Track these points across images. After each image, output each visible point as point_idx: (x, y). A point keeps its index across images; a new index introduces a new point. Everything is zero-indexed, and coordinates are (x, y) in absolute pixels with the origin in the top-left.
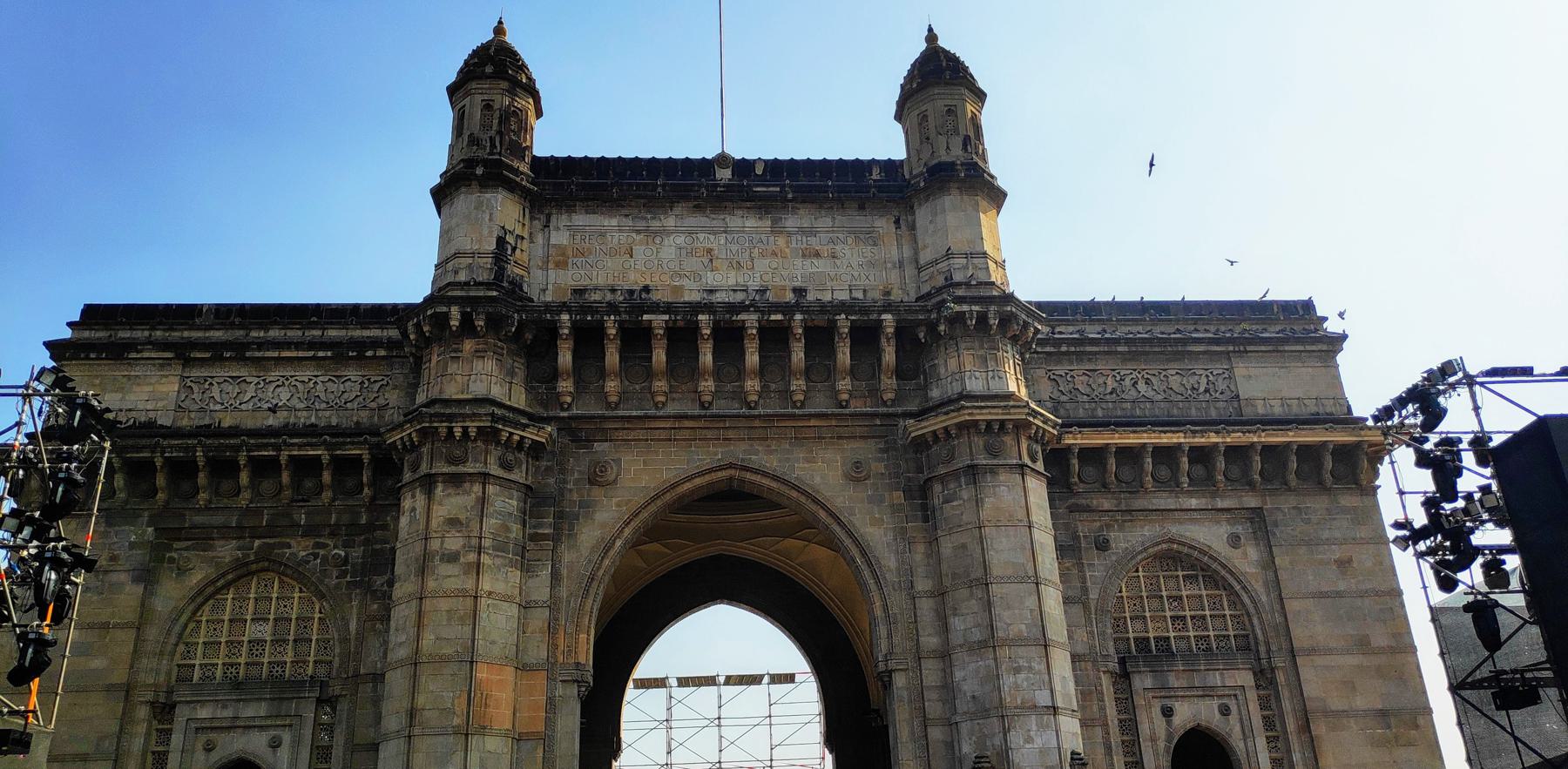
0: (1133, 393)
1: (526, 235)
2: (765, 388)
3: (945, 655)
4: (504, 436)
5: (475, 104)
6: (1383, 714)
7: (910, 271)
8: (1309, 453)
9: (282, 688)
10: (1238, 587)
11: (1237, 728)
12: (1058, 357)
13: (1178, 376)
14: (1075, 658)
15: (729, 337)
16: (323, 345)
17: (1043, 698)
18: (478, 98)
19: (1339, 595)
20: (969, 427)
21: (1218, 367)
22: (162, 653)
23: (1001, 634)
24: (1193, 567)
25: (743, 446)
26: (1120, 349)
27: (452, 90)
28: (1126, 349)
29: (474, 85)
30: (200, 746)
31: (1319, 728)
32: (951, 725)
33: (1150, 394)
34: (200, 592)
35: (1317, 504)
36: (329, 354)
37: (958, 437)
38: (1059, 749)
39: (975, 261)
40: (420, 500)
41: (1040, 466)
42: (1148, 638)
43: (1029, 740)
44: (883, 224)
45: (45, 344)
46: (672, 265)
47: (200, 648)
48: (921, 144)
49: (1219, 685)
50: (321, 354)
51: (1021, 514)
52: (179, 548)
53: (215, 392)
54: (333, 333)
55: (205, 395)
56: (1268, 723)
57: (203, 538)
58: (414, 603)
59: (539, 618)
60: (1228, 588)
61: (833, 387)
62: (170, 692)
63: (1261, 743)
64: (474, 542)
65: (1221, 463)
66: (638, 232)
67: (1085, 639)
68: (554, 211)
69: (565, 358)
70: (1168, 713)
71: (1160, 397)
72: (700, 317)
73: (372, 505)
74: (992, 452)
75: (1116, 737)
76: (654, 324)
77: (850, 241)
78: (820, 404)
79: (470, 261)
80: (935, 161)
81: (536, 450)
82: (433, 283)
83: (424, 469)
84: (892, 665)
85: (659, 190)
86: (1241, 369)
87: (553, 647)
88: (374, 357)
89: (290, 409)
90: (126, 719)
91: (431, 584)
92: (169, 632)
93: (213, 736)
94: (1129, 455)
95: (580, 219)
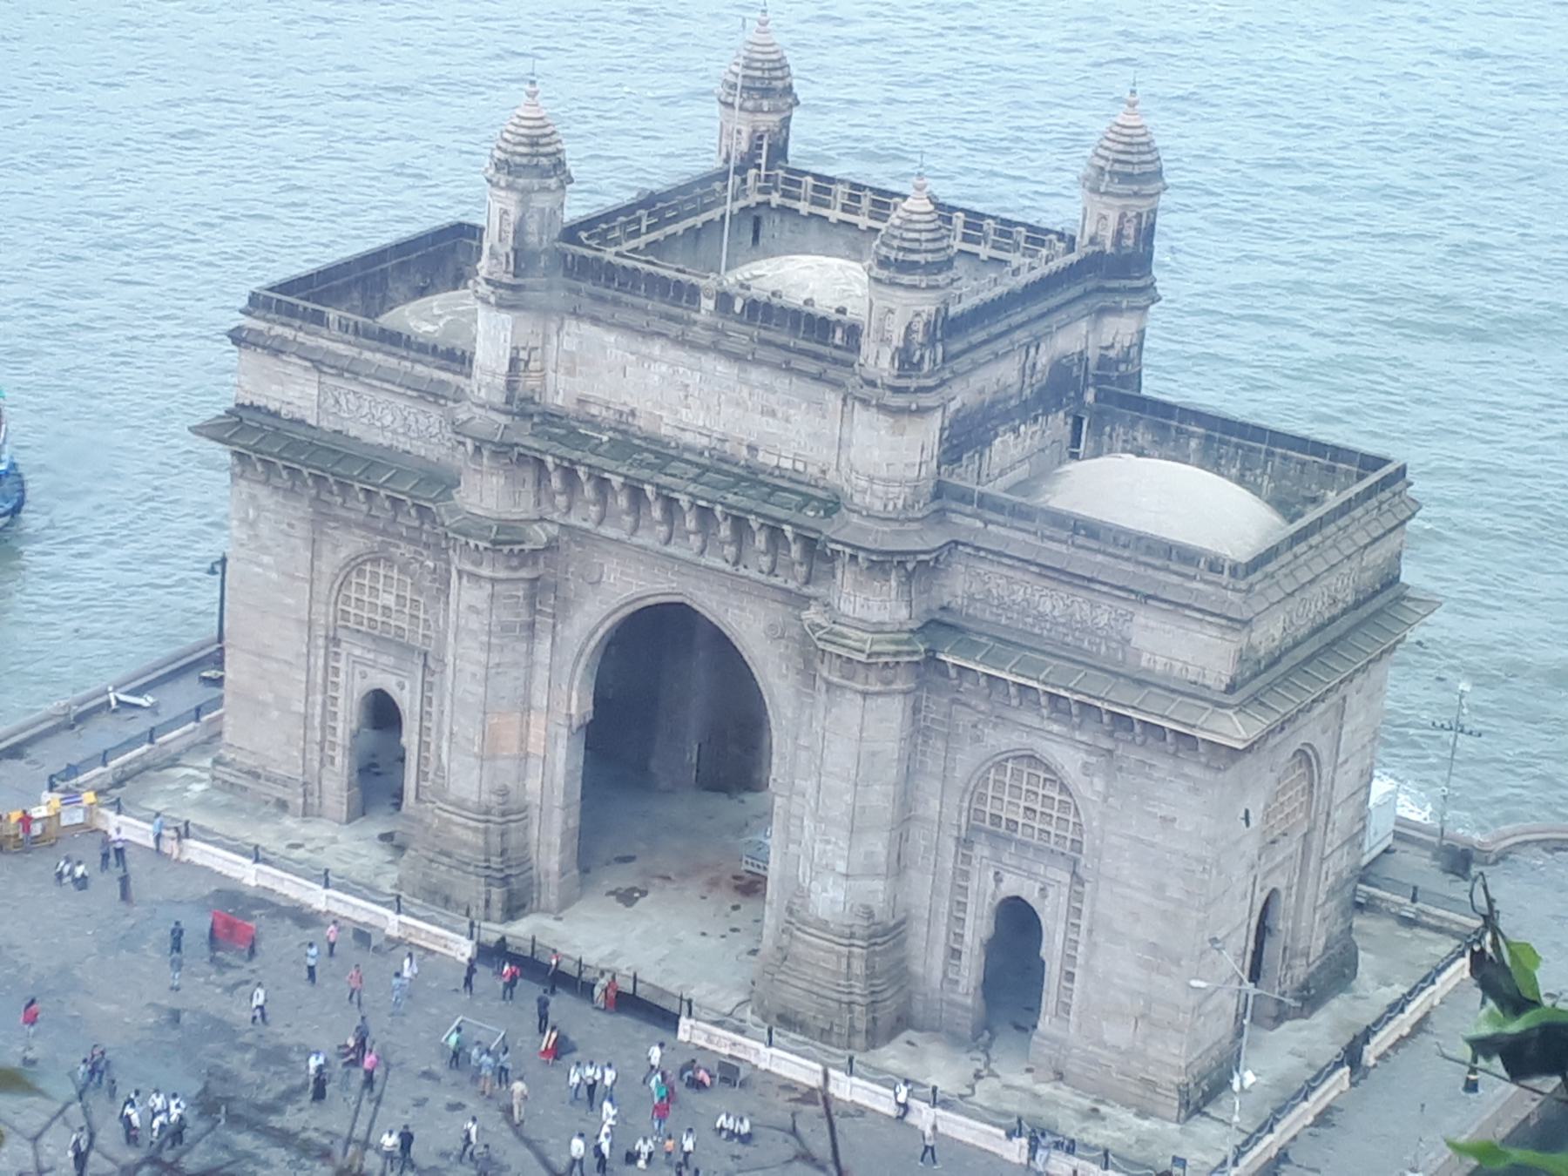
6: (1153, 948)
17: (841, 867)
19: (1153, 845)
21: (1124, 607)
31: (1100, 938)
63: (1061, 926)
70: (998, 879)
77: (804, 406)
86: (1140, 619)
95: (587, 328)
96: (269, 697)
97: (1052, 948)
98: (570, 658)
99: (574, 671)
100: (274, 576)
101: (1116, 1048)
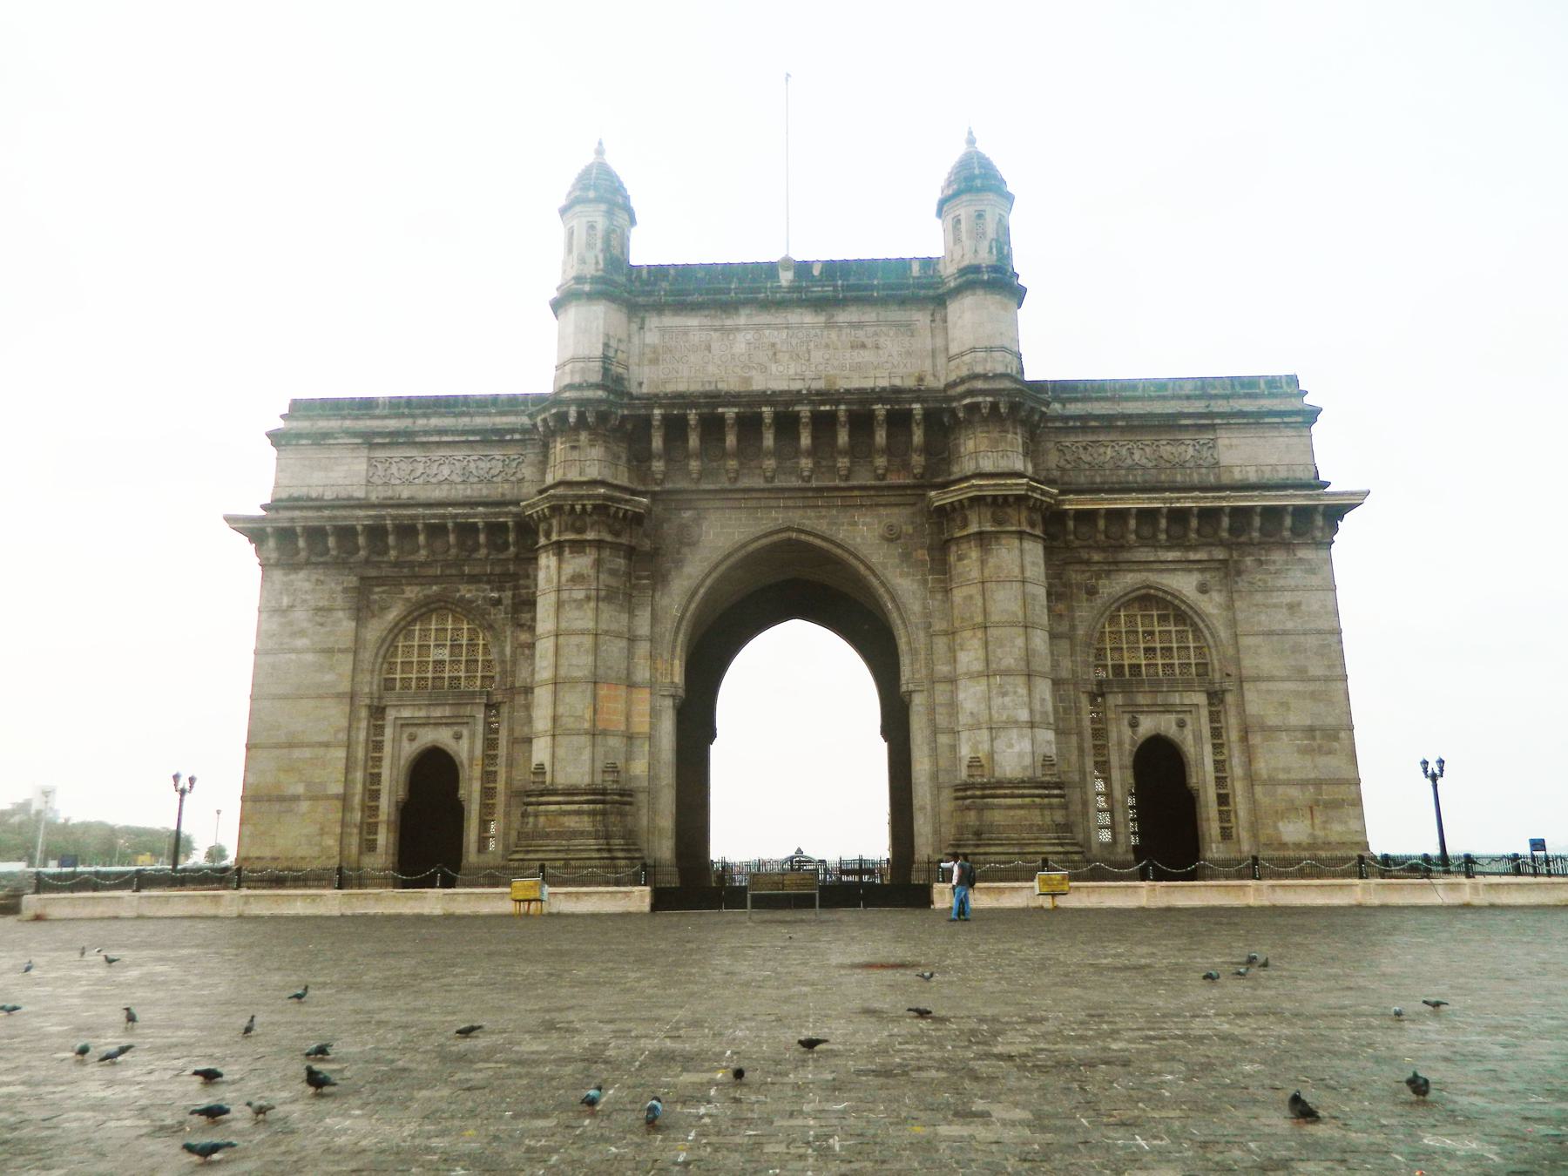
0: (1129, 462)
1: (624, 337)
2: (817, 464)
3: (952, 680)
4: (612, 510)
5: (580, 225)
6: (1310, 731)
7: (941, 360)
9: (461, 697)
10: (1201, 625)
11: (1190, 737)
12: (1068, 430)
13: (1169, 448)
14: (1057, 683)
16: (473, 432)
17: (1024, 715)
18: (584, 220)
19: (1285, 633)
20: (977, 501)
21: (1205, 437)
22: (372, 671)
23: (994, 666)
24: (1166, 608)
25: (800, 512)
26: (1119, 423)
27: (563, 211)
28: (1123, 423)
30: (405, 736)
31: (1256, 739)
32: (955, 733)
33: (1144, 461)
34: (397, 624)
35: (1278, 556)
36: (478, 438)
37: (971, 507)
38: (1033, 753)
39: (994, 354)
40: (553, 561)
41: (1038, 532)
42: (1122, 666)
44: (921, 318)
46: (742, 359)
47: (399, 667)
48: (955, 244)
49: (1178, 702)
50: (471, 438)
51: (1017, 571)
52: (378, 593)
53: (394, 469)
54: (480, 421)
55: (389, 472)
56: (1216, 733)
57: (395, 583)
58: (552, 640)
59: (643, 648)
60: (1194, 625)
61: (871, 462)
62: (380, 698)
63: (1208, 749)
64: (593, 593)
65: (1194, 523)
66: (716, 330)
67: (1070, 665)
68: (647, 315)
69: (657, 443)
70: (1134, 725)
71: (1150, 465)
72: (764, 409)
73: (517, 558)
74: (997, 521)
75: (1089, 743)
77: (891, 333)
78: (863, 478)
79: (582, 364)
80: (966, 263)
81: (637, 519)
82: (555, 381)
83: (554, 537)
84: (911, 687)
85: (733, 294)
86: (1224, 439)
87: (653, 669)
88: (511, 440)
89: (452, 482)
90: (352, 717)
91: (563, 625)
92: (377, 654)
93: (413, 730)
94: (1118, 516)
95: (670, 320)
96: (300, 789)
97: (1202, 775)
98: (667, 626)
99: (675, 640)
100: (310, 657)
101: (1298, 846)
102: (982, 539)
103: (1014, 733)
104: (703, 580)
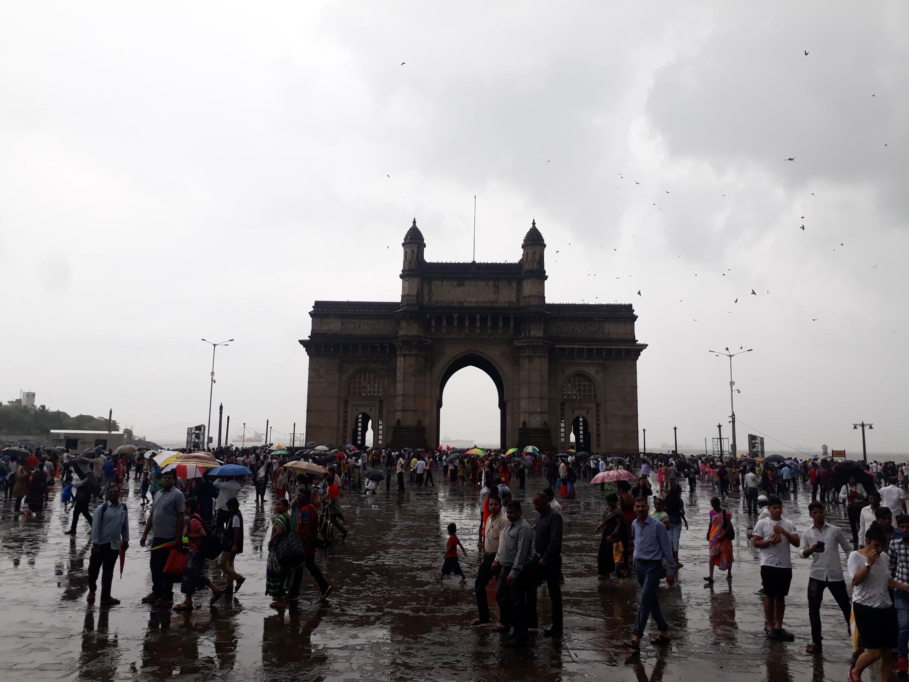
8: (619, 351)
10: (595, 382)
15: (473, 320)
17: (539, 410)
18: (411, 249)
27: (403, 245)
29: (408, 245)
40: (402, 359)
41: (547, 355)
43: (534, 419)
45: (309, 313)
53: (350, 326)
56: (598, 416)
60: (593, 382)
63: (595, 420)
70: (573, 413)
76: (455, 316)
102: (529, 357)
103: (536, 415)
104: (446, 365)
